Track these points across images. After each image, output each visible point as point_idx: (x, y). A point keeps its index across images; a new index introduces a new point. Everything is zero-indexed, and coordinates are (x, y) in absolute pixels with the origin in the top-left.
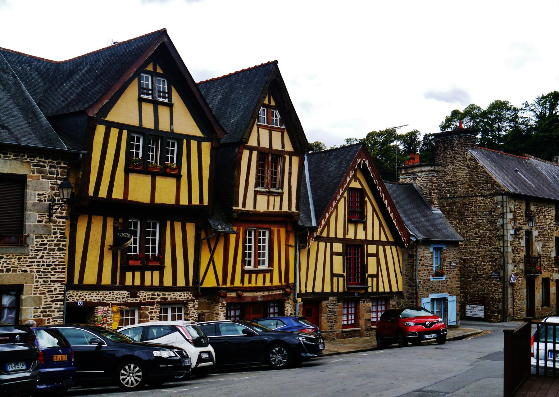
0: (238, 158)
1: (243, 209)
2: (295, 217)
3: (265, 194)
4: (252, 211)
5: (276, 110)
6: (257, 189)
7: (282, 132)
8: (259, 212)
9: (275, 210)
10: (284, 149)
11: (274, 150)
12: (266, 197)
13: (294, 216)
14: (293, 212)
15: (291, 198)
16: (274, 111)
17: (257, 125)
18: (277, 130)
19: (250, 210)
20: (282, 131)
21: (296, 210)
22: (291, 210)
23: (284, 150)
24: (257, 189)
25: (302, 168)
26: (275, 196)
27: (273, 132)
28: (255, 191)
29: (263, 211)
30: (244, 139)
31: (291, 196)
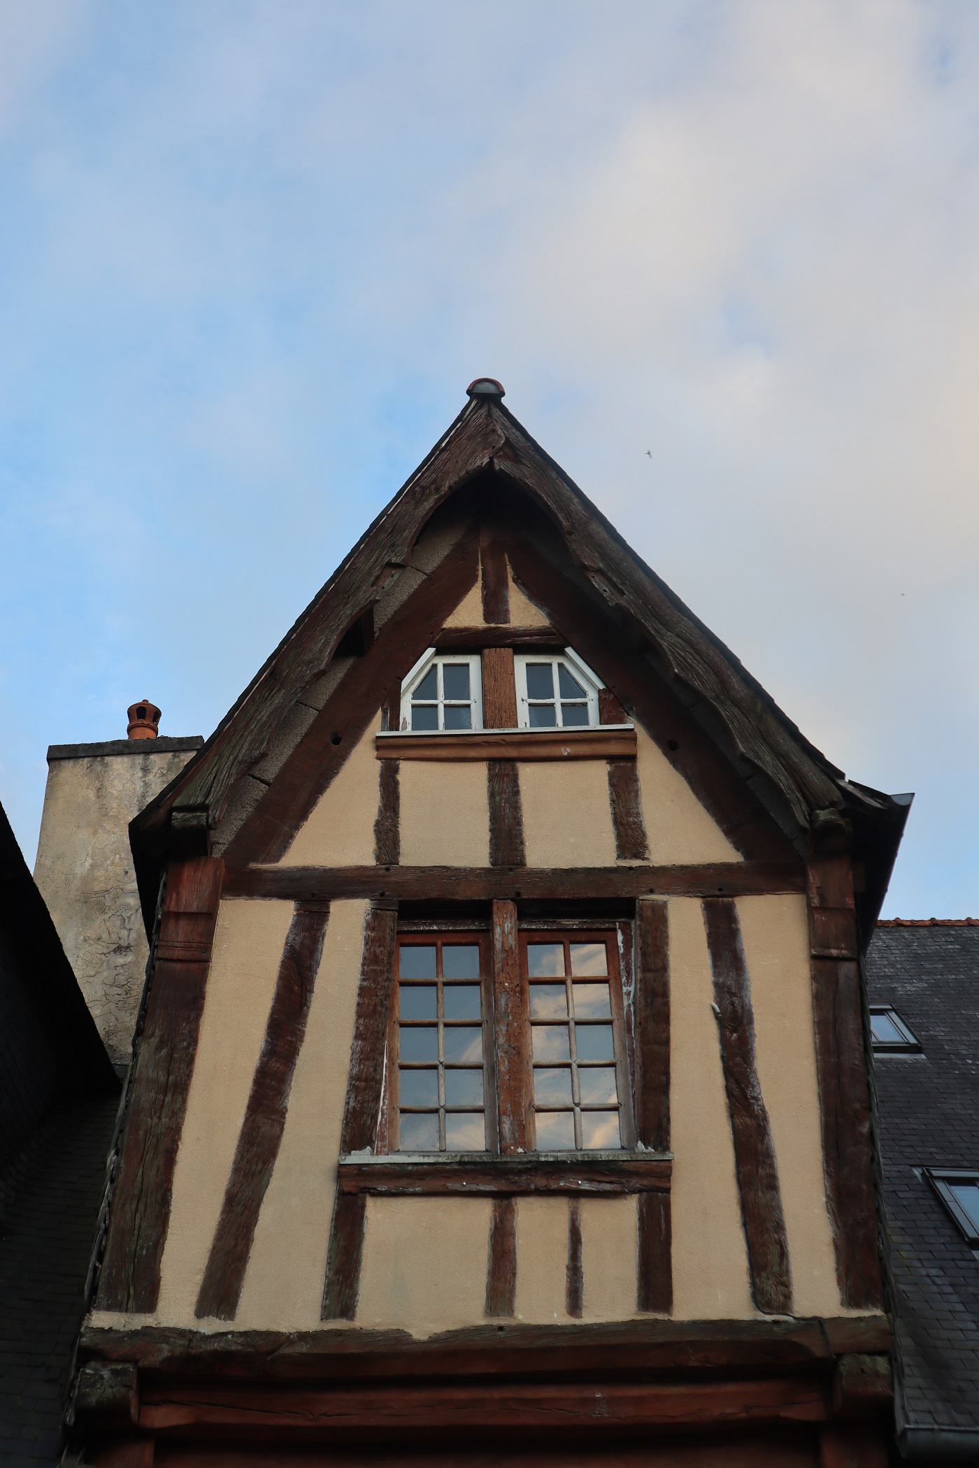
0: (177, 953)
1: (211, 1326)
2: (846, 1365)
3: (452, 1185)
4: (303, 1336)
5: (560, 651)
6: (360, 1157)
7: (611, 759)
8: (399, 1337)
9: (589, 1317)
10: (637, 856)
11: (540, 874)
12: (481, 1213)
13: (840, 1356)
14: (816, 1323)
15: (775, 1209)
16: (555, 661)
17: (381, 745)
18: (566, 751)
19: (286, 1325)
20: (615, 749)
21: (851, 1299)
22: (785, 1307)
23: (636, 863)
24: (360, 1157)
25: (847, 969)
26: (575, 1194)
27: (527, 773)
28: (342, 1172)
29: (438, 1328)
30: (181, 809)
31: (772, 1184)
